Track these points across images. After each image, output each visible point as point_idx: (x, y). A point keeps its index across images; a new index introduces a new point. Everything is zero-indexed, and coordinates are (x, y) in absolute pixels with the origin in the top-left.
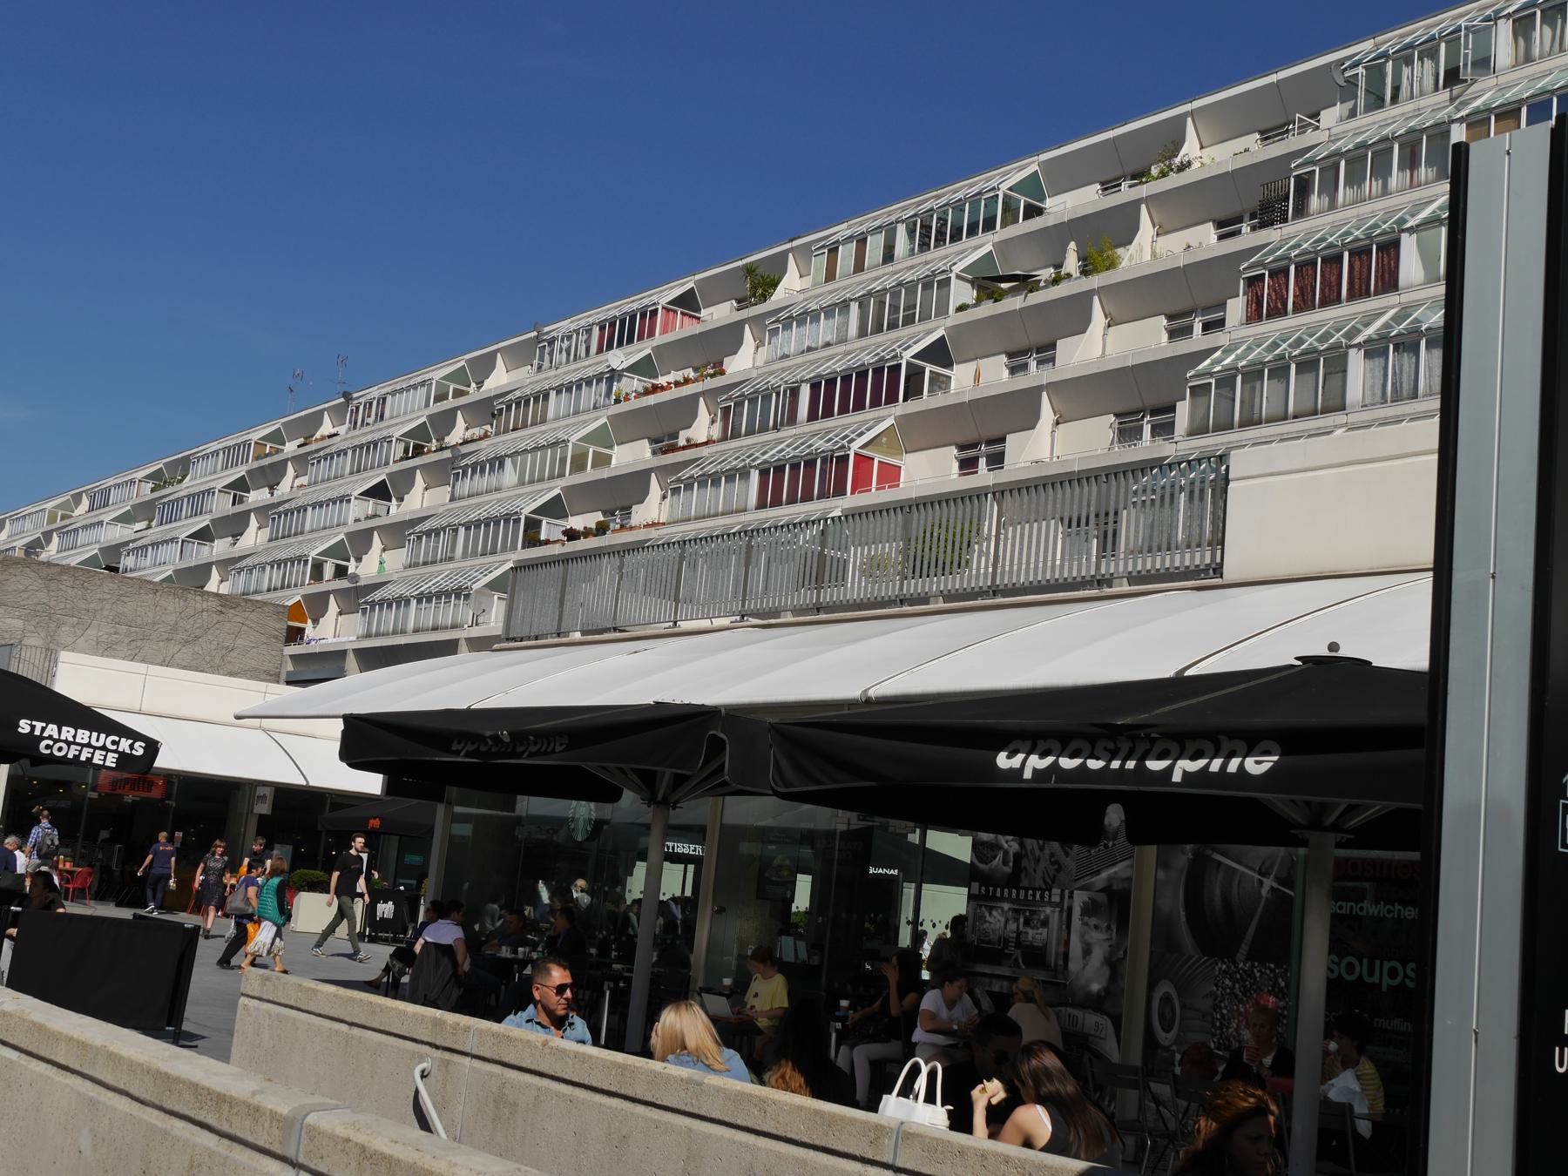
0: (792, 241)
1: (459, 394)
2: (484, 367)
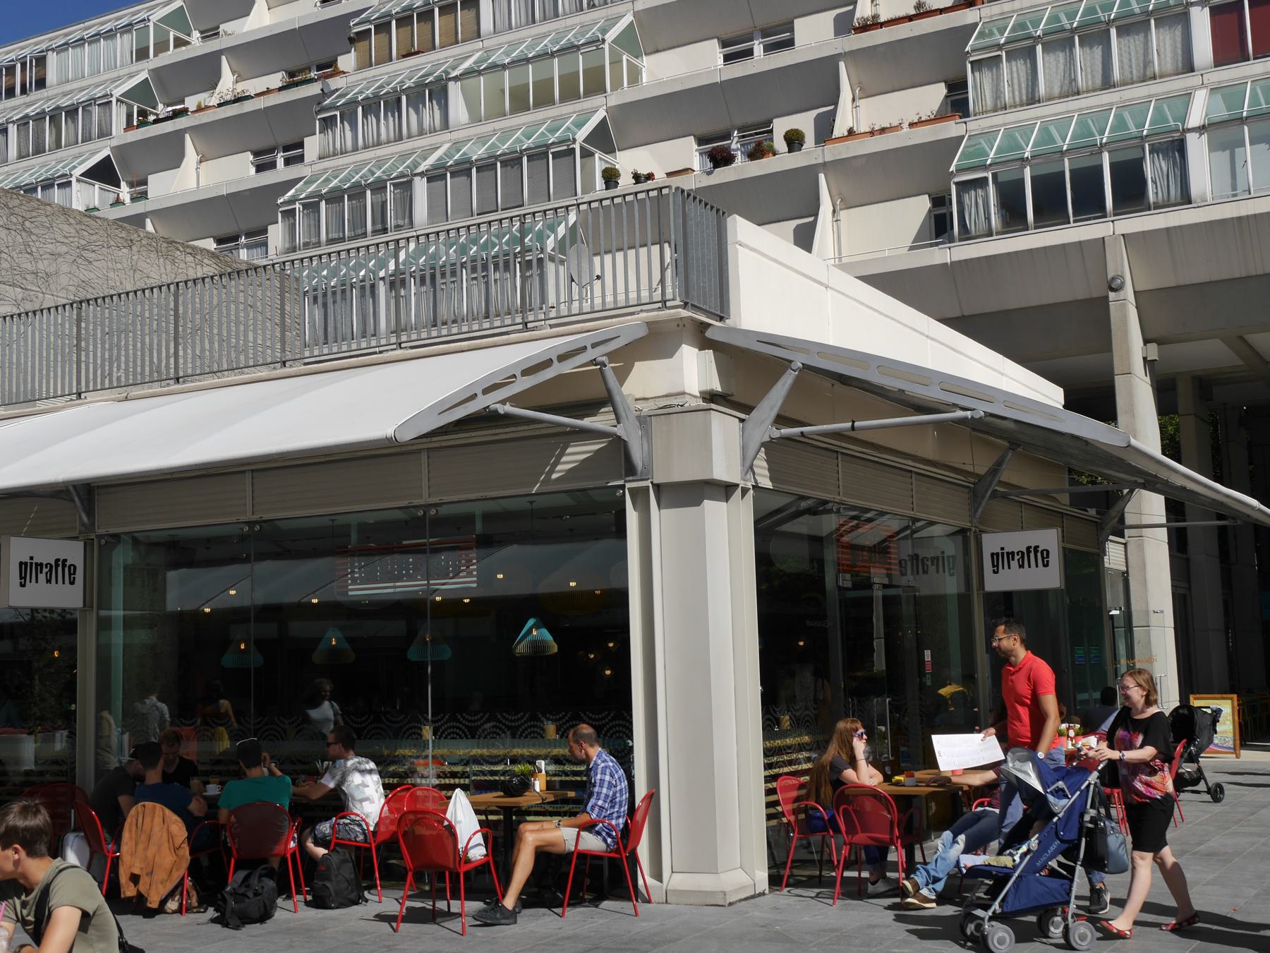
1: (179, 43)
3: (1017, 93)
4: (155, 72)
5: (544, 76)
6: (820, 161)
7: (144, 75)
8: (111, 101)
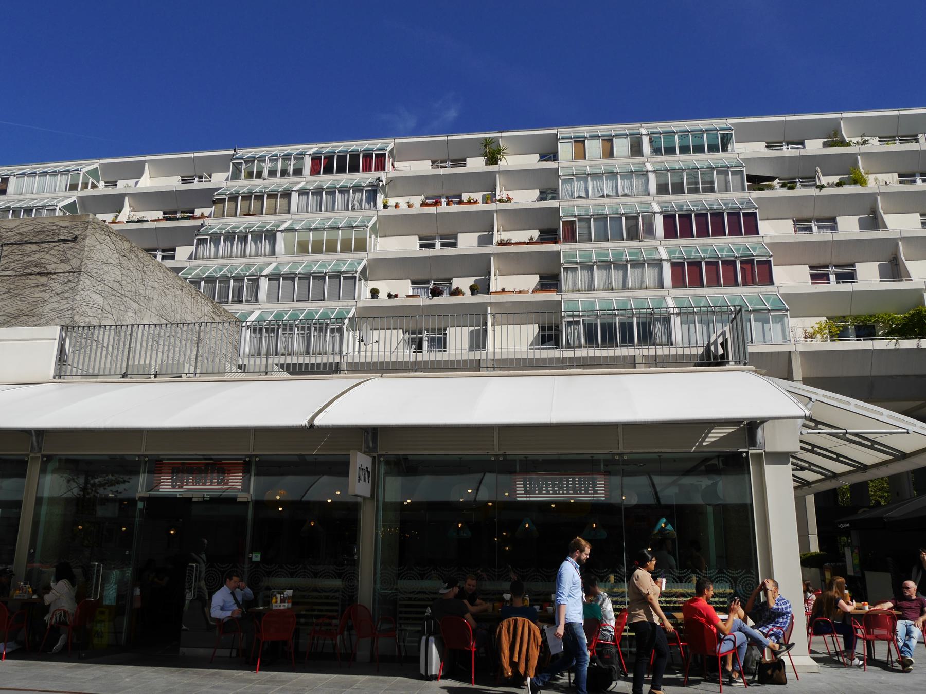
0: (501, 132)
1: (94, 186)
2: (136, 172)
3: (583, 285)
4: (82, 199)
5: (347, 237)
6: (489, 301)
7: (74, 199)
8: (56, 209)
